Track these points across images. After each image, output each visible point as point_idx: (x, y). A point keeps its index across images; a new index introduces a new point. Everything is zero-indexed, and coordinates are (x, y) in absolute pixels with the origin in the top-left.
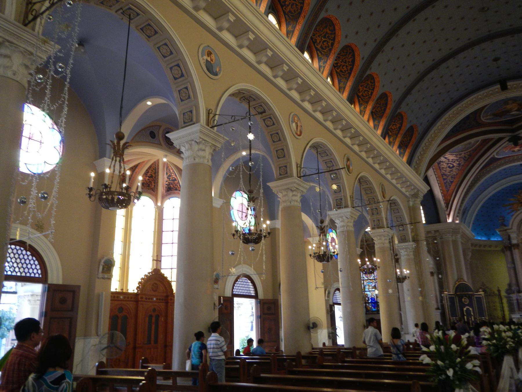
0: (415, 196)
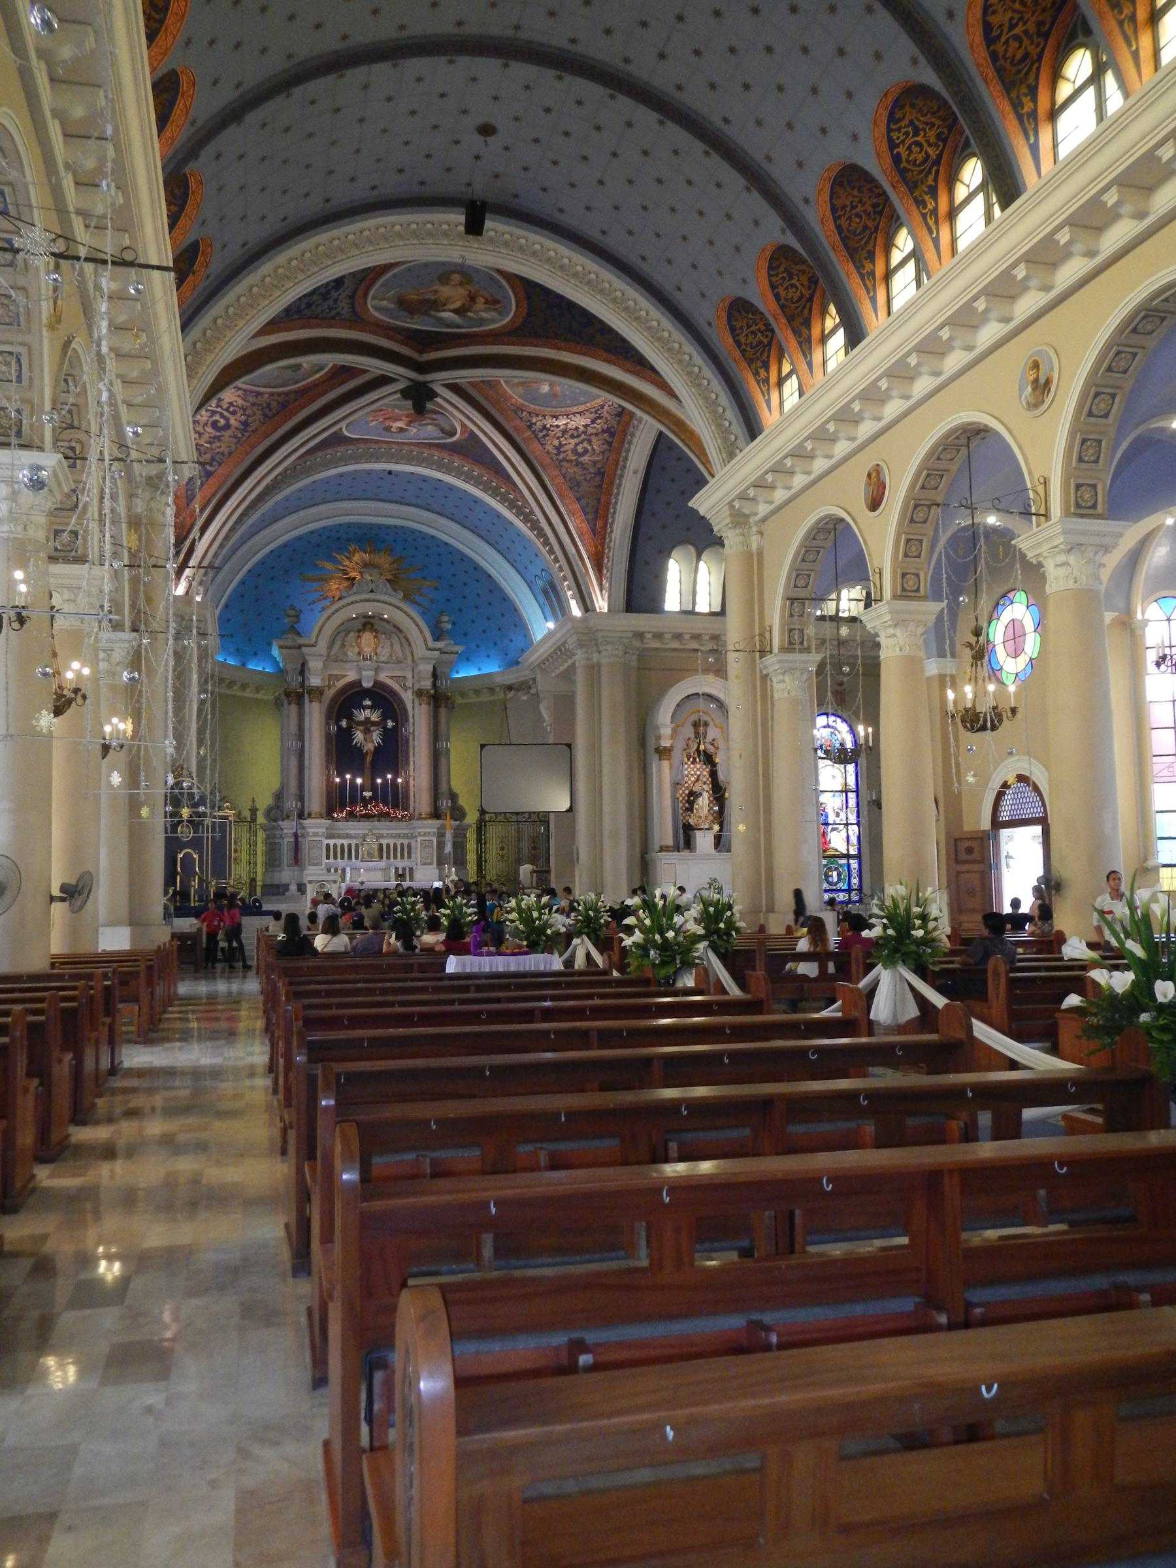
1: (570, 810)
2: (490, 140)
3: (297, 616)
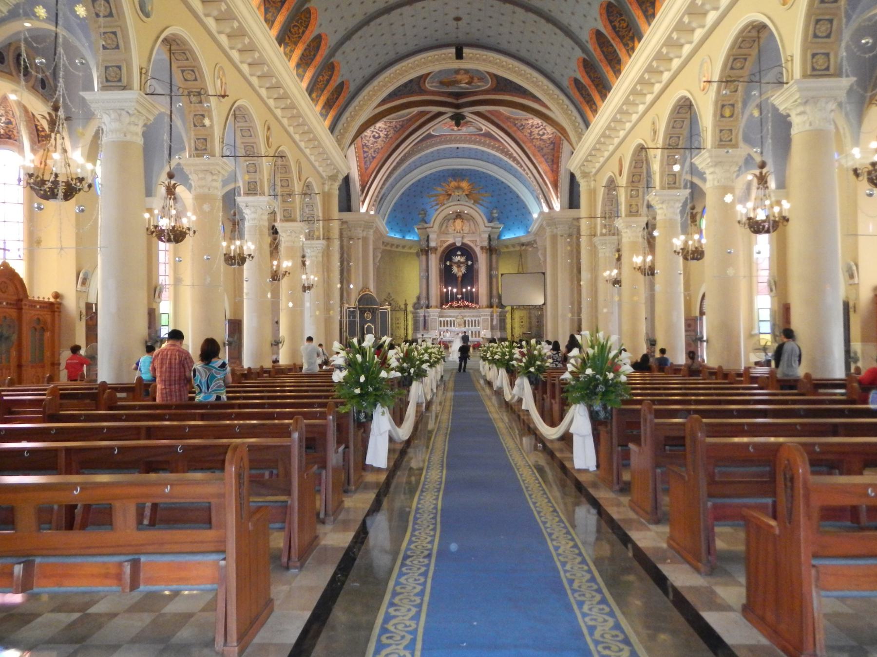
0: (333, 178)
1: (544, 304)
2: (460, 23)
3: (425, 214)
